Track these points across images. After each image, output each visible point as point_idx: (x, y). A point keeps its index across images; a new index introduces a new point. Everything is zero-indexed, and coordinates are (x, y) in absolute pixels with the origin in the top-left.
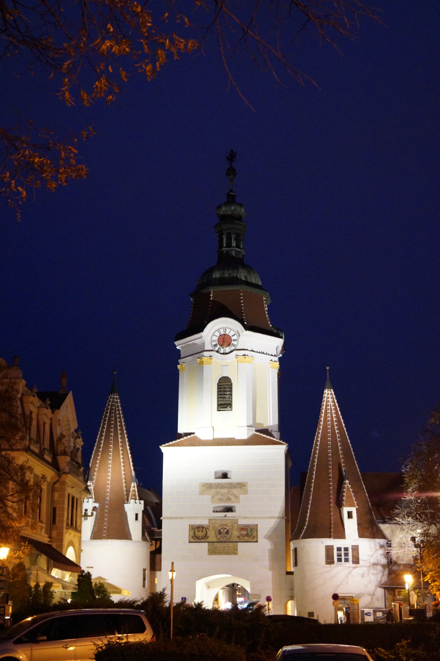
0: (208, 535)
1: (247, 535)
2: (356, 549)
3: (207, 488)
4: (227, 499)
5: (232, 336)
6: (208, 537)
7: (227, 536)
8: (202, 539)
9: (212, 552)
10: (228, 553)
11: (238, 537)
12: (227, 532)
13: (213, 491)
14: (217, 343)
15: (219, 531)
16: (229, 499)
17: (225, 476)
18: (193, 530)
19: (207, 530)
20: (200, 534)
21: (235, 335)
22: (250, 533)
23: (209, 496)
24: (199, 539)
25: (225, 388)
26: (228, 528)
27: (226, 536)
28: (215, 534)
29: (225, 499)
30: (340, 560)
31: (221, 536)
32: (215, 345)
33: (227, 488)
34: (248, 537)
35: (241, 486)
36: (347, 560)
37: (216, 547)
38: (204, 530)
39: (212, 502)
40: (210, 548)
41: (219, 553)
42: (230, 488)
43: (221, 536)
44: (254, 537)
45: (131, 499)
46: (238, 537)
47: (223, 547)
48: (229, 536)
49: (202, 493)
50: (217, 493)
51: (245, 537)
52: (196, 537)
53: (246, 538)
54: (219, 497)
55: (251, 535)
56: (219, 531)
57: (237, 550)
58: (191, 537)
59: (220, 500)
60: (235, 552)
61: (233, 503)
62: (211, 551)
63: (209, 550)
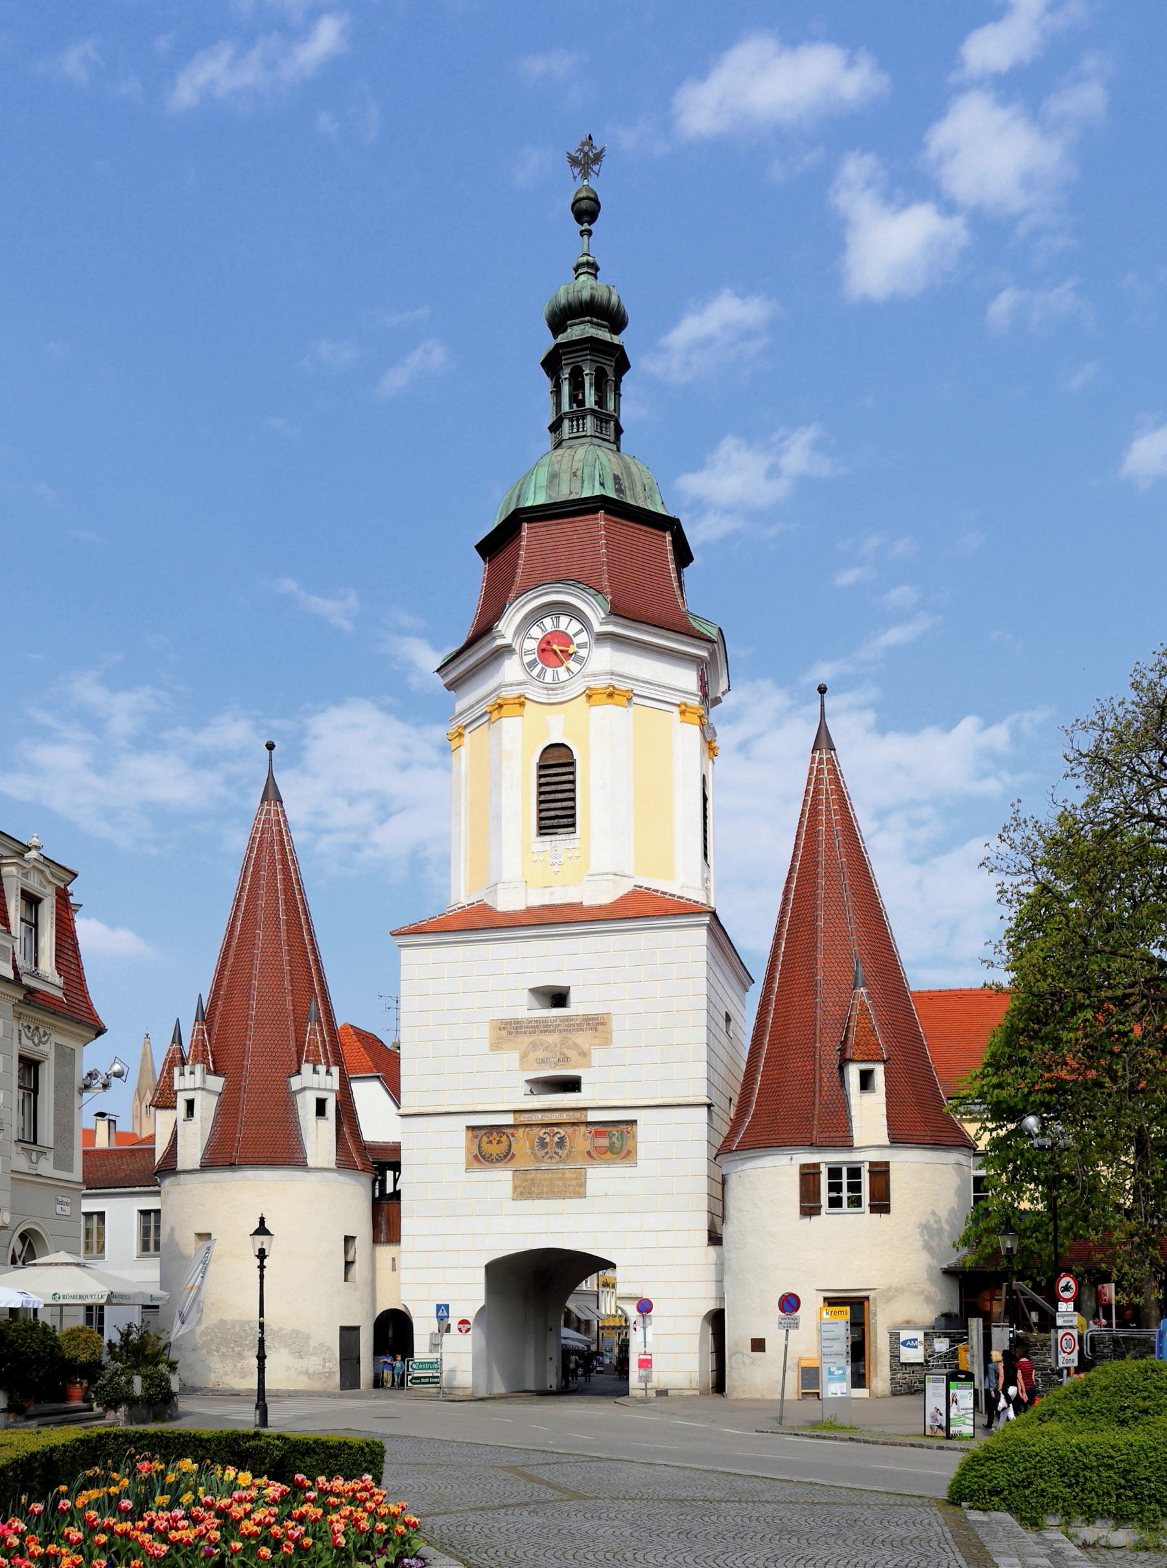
0: (513, 1150)
1: (611, 1149)
3: (509, 1033)
5: (575, 635)
6: (513, 1155)
7: (560, 1152)
9: (525, 1190)
11: (589, 1153)
13: (526, 1040)
14: (536, 656)
15: (542, 1139)
16: (564, 1060)
17: (558, 998)
18: (477, 1141)
20: (494, 1149)
21: (581, 631)
22: (618, 1144)
25: (557, 771)
27: (557, 1153)
32: (532, 664)
33: (559, 1031)
35: (596, 1023)
36: (856, 1202)
37: (532, 1180)
40: (519, 1183)
41: (539, 1197)
42: (566, 1030)
44: (629, 1152)
45: (307, 1061)
46: (589, 1153)
47: (551, 1180)
49: (496, 1046)
50: (534, 1046)
52: (484, 1157)
54: (540, 1054)
55: (622, 1146)
56: (542, 1139)
57: (583, 1185)
58: (471, 1157)
59: (542, 1061)
60: (578, 1190)
61: (575, 1067)
63: (515, 1188)
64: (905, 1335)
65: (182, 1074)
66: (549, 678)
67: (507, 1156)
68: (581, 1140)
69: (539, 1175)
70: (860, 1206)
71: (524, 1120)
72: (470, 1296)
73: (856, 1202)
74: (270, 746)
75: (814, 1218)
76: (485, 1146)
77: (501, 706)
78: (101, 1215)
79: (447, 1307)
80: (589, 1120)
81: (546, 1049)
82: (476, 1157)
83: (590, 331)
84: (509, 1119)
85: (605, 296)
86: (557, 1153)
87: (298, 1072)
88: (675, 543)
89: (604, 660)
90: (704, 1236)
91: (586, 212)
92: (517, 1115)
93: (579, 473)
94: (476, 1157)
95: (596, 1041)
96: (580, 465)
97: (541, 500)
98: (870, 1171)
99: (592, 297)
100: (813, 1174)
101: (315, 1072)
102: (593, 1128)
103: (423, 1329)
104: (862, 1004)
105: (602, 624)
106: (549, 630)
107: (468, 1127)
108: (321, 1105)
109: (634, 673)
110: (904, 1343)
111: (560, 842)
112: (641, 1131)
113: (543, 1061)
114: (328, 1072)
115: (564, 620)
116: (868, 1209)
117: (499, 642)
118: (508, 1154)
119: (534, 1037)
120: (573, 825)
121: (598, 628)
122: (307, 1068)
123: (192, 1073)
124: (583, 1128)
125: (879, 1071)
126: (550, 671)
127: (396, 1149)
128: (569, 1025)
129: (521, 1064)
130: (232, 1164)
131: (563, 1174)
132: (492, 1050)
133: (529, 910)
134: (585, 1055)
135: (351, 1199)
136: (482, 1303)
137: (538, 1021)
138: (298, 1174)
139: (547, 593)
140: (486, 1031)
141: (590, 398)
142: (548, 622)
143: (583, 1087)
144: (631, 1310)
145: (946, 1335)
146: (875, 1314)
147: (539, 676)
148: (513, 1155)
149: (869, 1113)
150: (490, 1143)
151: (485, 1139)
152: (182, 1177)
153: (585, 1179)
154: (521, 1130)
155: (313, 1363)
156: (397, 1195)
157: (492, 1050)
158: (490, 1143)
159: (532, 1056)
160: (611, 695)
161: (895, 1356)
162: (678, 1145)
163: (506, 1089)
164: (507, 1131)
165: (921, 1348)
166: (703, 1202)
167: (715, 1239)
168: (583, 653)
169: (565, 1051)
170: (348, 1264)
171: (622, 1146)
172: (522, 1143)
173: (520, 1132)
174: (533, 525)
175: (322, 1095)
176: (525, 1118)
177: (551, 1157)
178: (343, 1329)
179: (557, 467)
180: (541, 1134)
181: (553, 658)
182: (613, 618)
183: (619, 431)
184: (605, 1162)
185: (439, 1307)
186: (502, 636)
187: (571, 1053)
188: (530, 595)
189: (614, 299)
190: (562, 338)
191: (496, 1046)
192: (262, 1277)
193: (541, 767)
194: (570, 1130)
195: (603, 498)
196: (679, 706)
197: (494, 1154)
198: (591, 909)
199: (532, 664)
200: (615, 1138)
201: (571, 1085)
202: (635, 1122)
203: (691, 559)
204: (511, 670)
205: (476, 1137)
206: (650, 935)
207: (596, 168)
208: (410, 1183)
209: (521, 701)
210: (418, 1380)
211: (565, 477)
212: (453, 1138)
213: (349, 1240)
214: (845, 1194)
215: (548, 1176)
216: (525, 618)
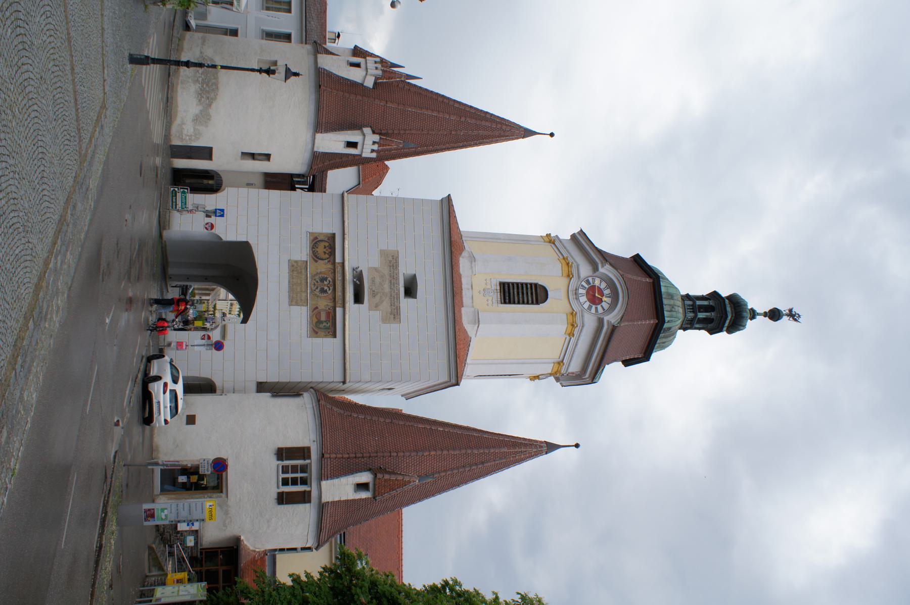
1: (319, 322)
2: (304, 498)
3: (390, 262)
6: (316, 261)
9: (295, 268)
10: (291, 289)
11: (317, 308)
13: (386, 271)
15: (326, 279)
16: (374, 294)
22: (322, 326)
28: (321, 273)
30: (285, 470)
35: (395, 315)
39: (370, 269)
41: (291, 277)
44: (316, 333)
46: (317, 308)
49: (383, 253)
50: (382, 276)
53: (315, 320)
54: (378, 280)
56: (326, 279)
57: (297, 305)
60: (294, 301)
63: (296, 262)
65: (376, 62)
66: (581, 291)
67: (316, 257)
68: (324, 303)
69: (303, 276)
70: (283, 484)
72: (229, 231)
74: (552, 135)
76: (323, 244)
78: (289, 11)
79: (222, 216)
81: (380, 284)
82: (316, 238)
84: (338, 259)
87: (374, 132)
88: (634, 359)
89: (590, 323)
90: (262, 379)
91: (774, 315)
97: (663, 289)
101: (374, 143)
103: (209, 201)
104: (409, 482)
105: (608, 321)
107: (334, 234)
109: (582, 338)
112: (329, 341)
114: (373, 151)
117: (600, 266)
120: (505, 303)
121: (606, 318)
122: (376, 138)
123: (377, 68)
124: (331, 304)
126: (584, 292)
127: (323, 190)
133: (460, 276)
136: (224, 239)
137: (397, 279)
140: (392, 248)
141: (701, 315)
142: (607, 292)
143: (357, 305)
144: (216, 336)
150: (325, 247)
151: (327, 244)
152: (312, 58)
155: (189, 129)
156: (294, 189)
158: (325, 247)
160: (573, 325)
163: (358, 255)
164: (332, 258)
166: (284, 379)
167: (262, 387)
168: (593, 310)
169: (379, 295)
170: (253, 156)
172: (323, 267)
173: (330, 266)
175: (359, 146)
176: (339, 269)
178: (211, 149)
182: (611, 327)
183: (685, 329)
184: (311, 318)
185: (223, 210)
186: (603, 266)
187: (378, 297)
188: (623, 282)
190: (727, 301)
191: (383, 253)
192: (253, 70)
193: (536, 285)
194: (331, 297)
195: (663, 322)
198: (460, 312)
199: (588, 282)
200: (326, 324)
201: (358, 299)
202: (335, 336)
203: (626, 366)
204: (585, 270)
206: (445, 347)
208: (300, 196)
209: (569, 276)
210: (175, 194)
211: (672, 302)
212: (327, 225)
213: (267, 157)
215: (303, 282)
216: (611, 279)
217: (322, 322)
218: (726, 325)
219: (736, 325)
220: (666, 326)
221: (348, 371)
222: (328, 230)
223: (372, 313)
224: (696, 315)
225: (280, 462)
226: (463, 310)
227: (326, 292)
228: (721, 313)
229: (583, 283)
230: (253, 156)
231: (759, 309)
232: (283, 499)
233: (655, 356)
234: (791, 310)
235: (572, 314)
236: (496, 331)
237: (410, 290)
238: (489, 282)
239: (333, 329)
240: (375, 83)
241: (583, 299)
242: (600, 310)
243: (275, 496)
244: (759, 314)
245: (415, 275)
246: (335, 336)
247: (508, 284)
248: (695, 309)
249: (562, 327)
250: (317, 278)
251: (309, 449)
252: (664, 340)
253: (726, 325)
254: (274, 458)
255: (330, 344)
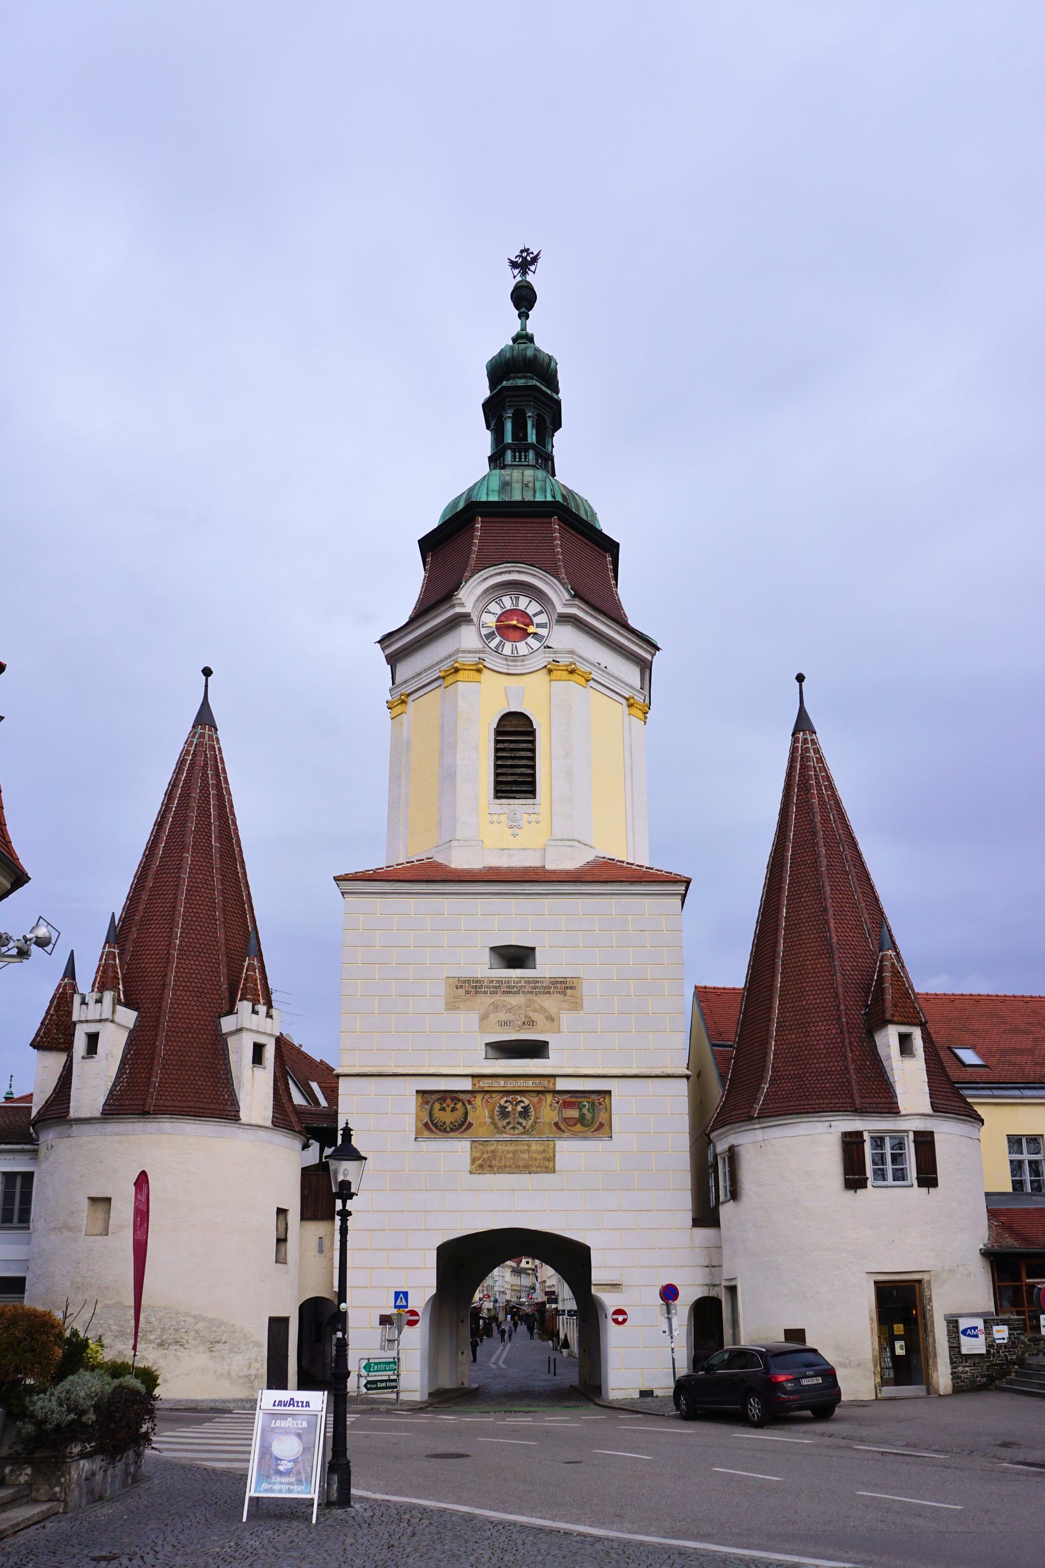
0: (469, 1119)
1: (581, 1120)
2: (925, 1142)
3: (467, 992)
4: (524, 1023)
5: (535, 615)
6: (470, 1125)
8: (452, 1130)
9: (483, 1164)
10: (526, 1169)
11: (556, 1124)
12: (525, 1113)
13: (487, 1000)
15: (503, 1108)
16: (530, 1023)
19: (468, 1107)
20: (447, 1117)
21: (541, 612)
22: (589, 1116)
23: (475, 1017)
24: (445, 1131)
25: (515, 739)
26: (527, 1102)
27: (521, 1124)
28: (492, 1117)
29: (520, 1023)
30: (880, 1174)
31: (508, 1123)
32: (490, 636)
34: (583, 1125)
37: (493, 1152)
38: (459, 1105)
39: (483, 1030)
40: (478, 1155)
41: (503, 1169)
42: (531, 992)
43: (508, 1123)
44: (601, 1125)
46: (556, 1124)
47: (514, 1152)
48: (530, 1122)
49: (452, 1006)
50: (496, 1007)
51: (575, 1125)
52: (435, 1125)
54: (503, 1016)
55: (593, 1118)
56: (503, 1108)
58: (420, 1125)
59: (505, 1024)
60: (547, 1164)
61: (541, 1032)
62: (478, 1162)
63: (473, 1161)
64: (964, 1324)
67: (462, 1126)
68: (548, 1112)
71: (483, 1086)
73: (900, 1175)
75: (860, 1191)
76: (438, 1114)
77: (457, 670)
79: (406, 1294)
80: (557, 1088)
82: (426, 1125)
83: (535, 382)
84: (467, 1085)
85: (546, 359)
86: (521, 1124)
89: (565, 638)
91: (524, 298)
92: (476, 1080)
93: (531, 485)
94: (426, 1125)
95: (565, 1005)
96: (531, 479)
98: (914, 1141)
99: (535, 357)
100: (857, 1143)
101: (255, 1012)
102: (561, 1098)
106: (508, 608)
107: (417, 1092)
108: (258, 1050)
110: (964, 1332)
111: (517, 806)
113: (506, 1023)
115: (523, 603)
116: (915, 1183)
118: (463, 1123)
119: (495, 998)
121: (560, 609)
124: (549, 1098)
125: (917, 1033)
128: (536, 988)
129: (480, 1026)
130: (148, 1113)
131: (529, 1146)
132: (447, 1009)
134: (553, 1020)
135: (286, 1159)
138: (227, 1129)
139: (509, 572)
140: (441, 989)
141: (532, 437)
145: (1004, 1322)
146: (930, 1300)
147: (497, 647)
148: (470, 1125)
149: (909, 1078)
150: (443, 1112)
151: (437, 1106)
153: (554, 1152)
154: (479, 1097)
157: (447, 1009)
158: (443, 1112)
159: (494, 1018)
161: (955, 1348)
162: (655, 1121)
163: (461, 1052)
164: (462, 1096)
165: (982, 1337)
169: (531, 1014)
170: (281, 1241)
171: (593, 1118)
173: (478, 1100)
174: (487, 520)
175: (261, 1040)
176: (485, 1084)
177: (514, 1128)
179: (508, 478)
180: (502, 1102)
181: (512, 634)
185: (397, 1294)
187: (535, 1016)
189: (553, 363)
191: (452, 1006)
193: (498, 732)
194: (535, 1100)
196: (627, 699)
197: (448, 1122)
198: (554, 872)
199: (490, 636)
200: (586, 1111)
201: (537, 1050)
202: (609, 1092)
205: (427, 1103)
207: (532, 268)
211: (517, 487)
212: (403, 1106)
214: (889, 1167)
217: (582, 1116)
218: (549, 392)
219: (543, 371)
220: (559, 498)
221: (669, 1071)
222: (411, 1104)
223: (564, 1027)
224: (532, 446)
225: (869, 1183)
226: (549, 866)
227: (526, 1109)
228: (523, 397)
229: (493, 644)
230: (281, 1241)
231: (515, 327)
232: (928, 1178)
233: (608, 526)
234: (514, 265)
235: (550, 671)
236: (584, 810)
237: (516, 957)
238: (495, 818)
239: (593, 1097)
240: (127, 1005)
241: (522, 648)
242: (542, 619)
243: (924, 1190)
244: (524, 329)
245: (492, 949)
246: (609, 1092)
247: (497, 783)
248: (520, 446)
249: (570, 689)
250: (501, 1124)
251: (846, 1135)
252: (582, 509)
253: (549, 392)
254: (861, 1192)
255: (624, 1101)
